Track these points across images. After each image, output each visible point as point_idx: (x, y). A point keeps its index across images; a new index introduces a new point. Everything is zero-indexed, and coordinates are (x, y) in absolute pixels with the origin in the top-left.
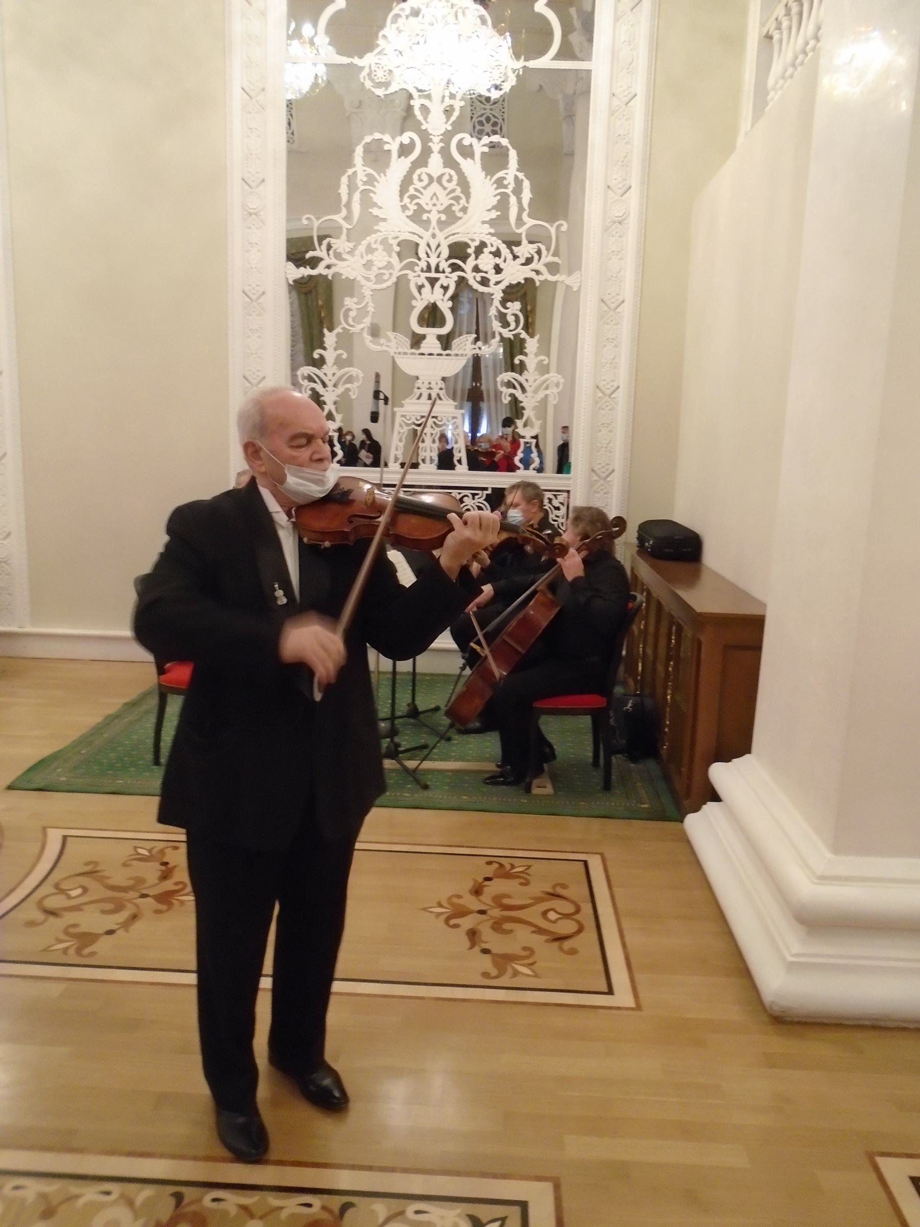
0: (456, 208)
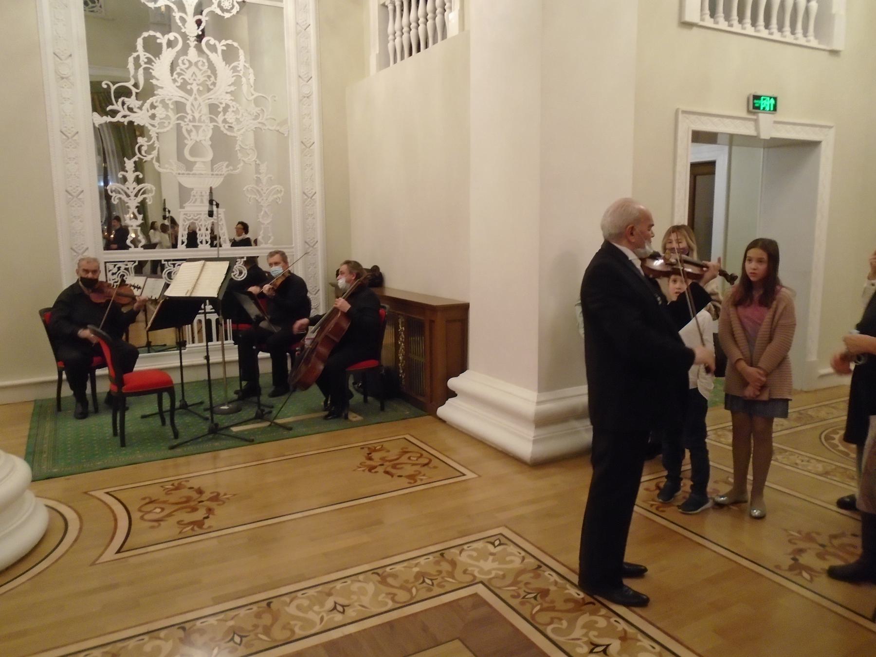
0: (209, 83)
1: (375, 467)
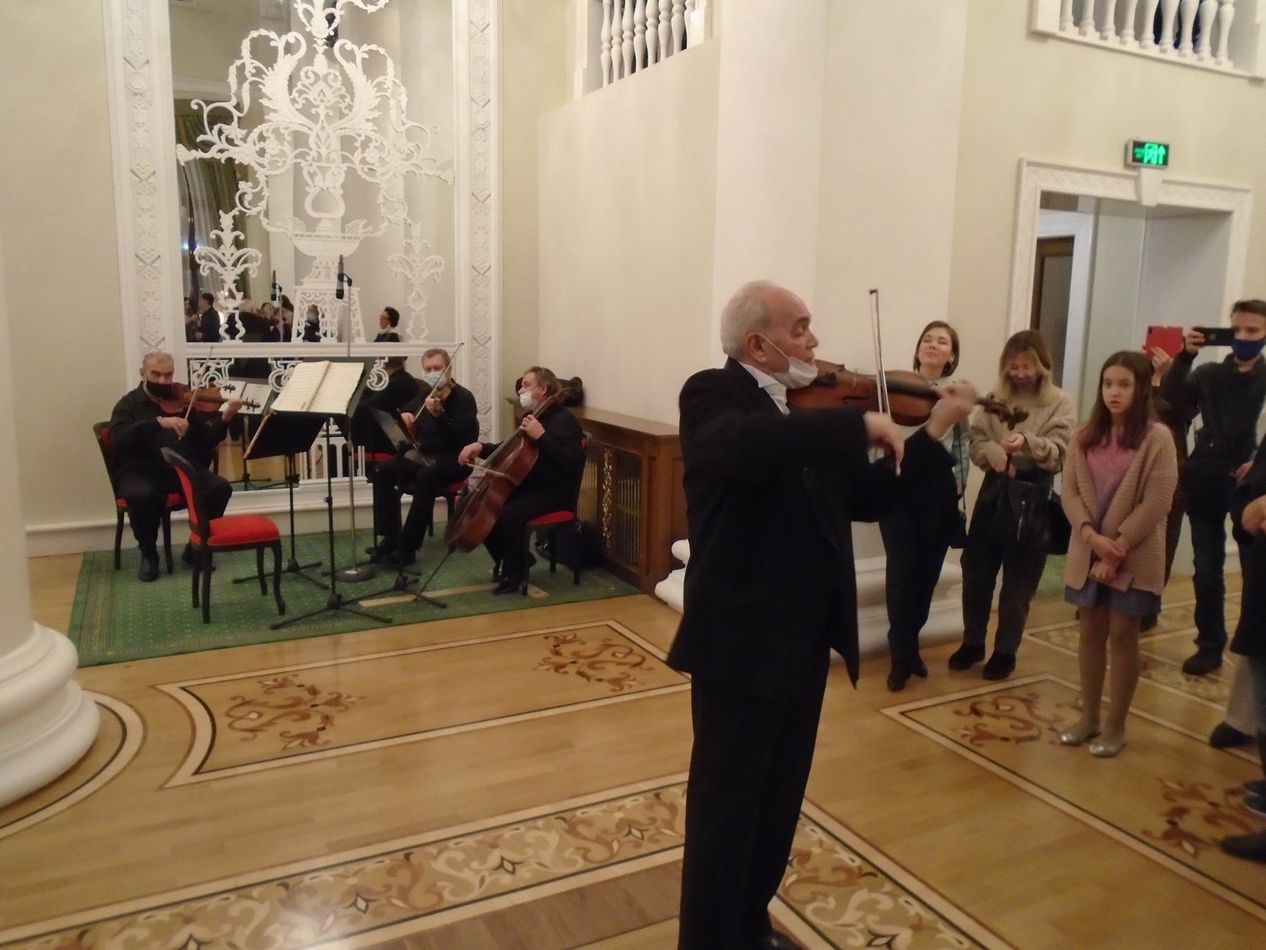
0: (342, 106)
1: (564, 666)
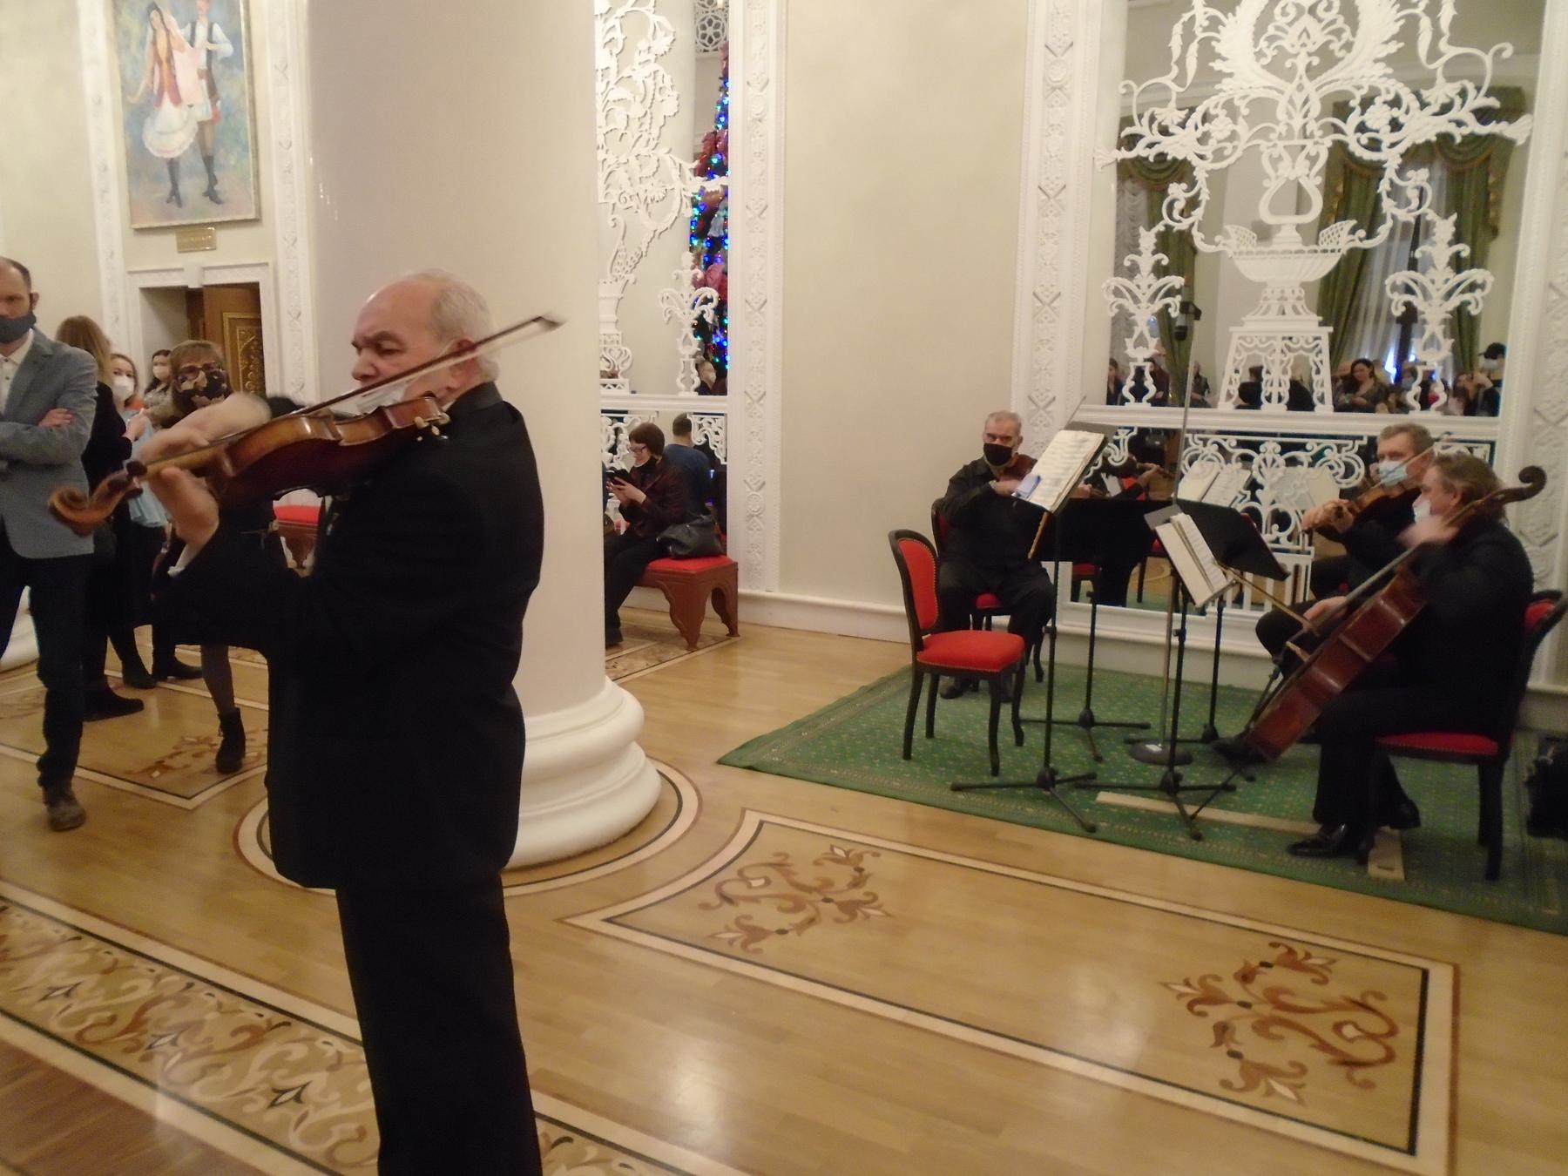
0: (1335, 46)
